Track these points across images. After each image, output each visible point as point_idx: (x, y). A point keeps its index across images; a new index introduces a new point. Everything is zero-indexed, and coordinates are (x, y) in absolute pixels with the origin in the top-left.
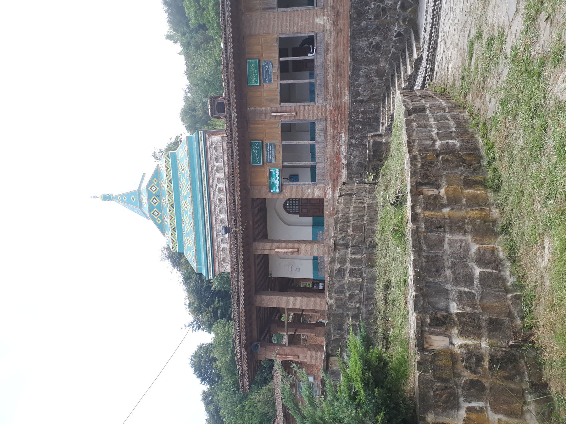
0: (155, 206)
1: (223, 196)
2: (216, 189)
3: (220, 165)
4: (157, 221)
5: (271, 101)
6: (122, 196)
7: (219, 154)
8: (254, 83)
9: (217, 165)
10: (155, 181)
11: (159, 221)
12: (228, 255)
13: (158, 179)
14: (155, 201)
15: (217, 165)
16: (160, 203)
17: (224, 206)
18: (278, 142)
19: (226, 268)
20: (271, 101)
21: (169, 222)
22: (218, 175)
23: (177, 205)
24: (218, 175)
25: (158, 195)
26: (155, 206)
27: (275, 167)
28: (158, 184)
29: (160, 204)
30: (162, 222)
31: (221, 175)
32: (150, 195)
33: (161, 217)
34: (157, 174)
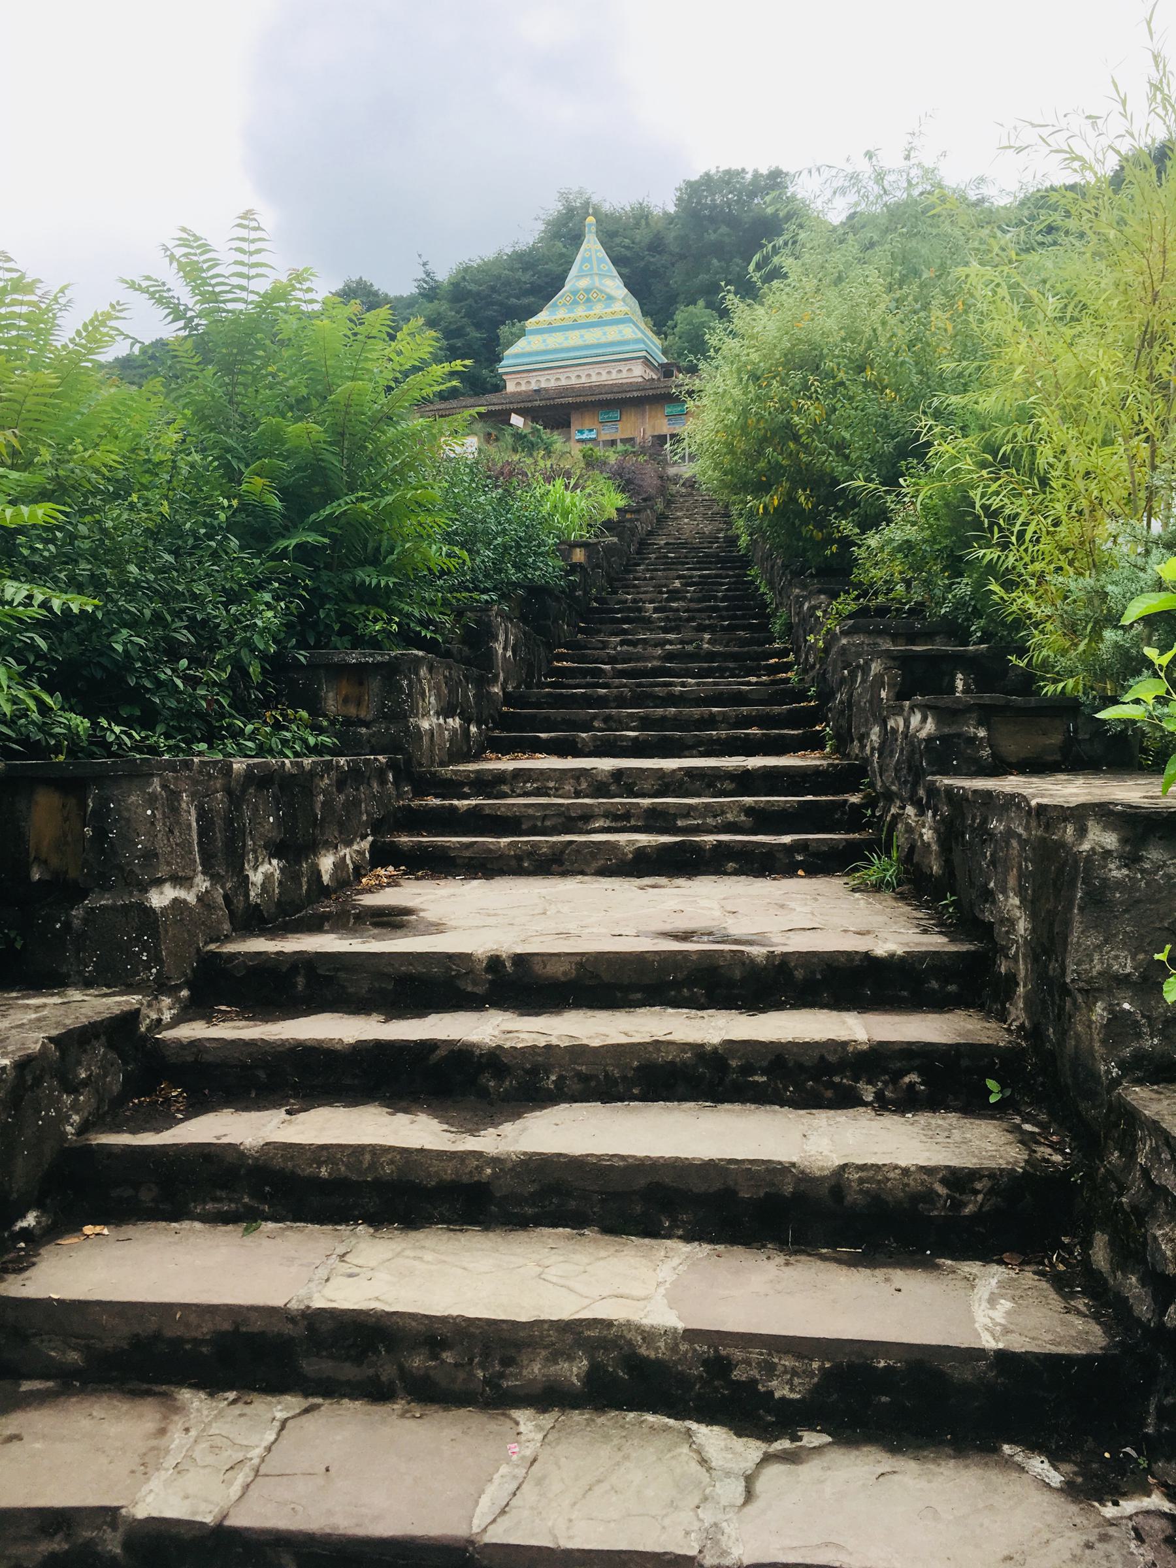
1: (583, 380)
2: (591, 372)
3: (614, 375)
5: (654, 427)
7: (625, 374)
8: (668, 410)
9: (614, 372)
12: (523, 388)
15: (614, 372)
17: (574, 381)
18: (618, 436)
19: (511, 387)
20: (654, 427)
22: (604, 373)
24: (604, 373)
27: (597, 433)
29: (578, 303)
31: (604, 377)
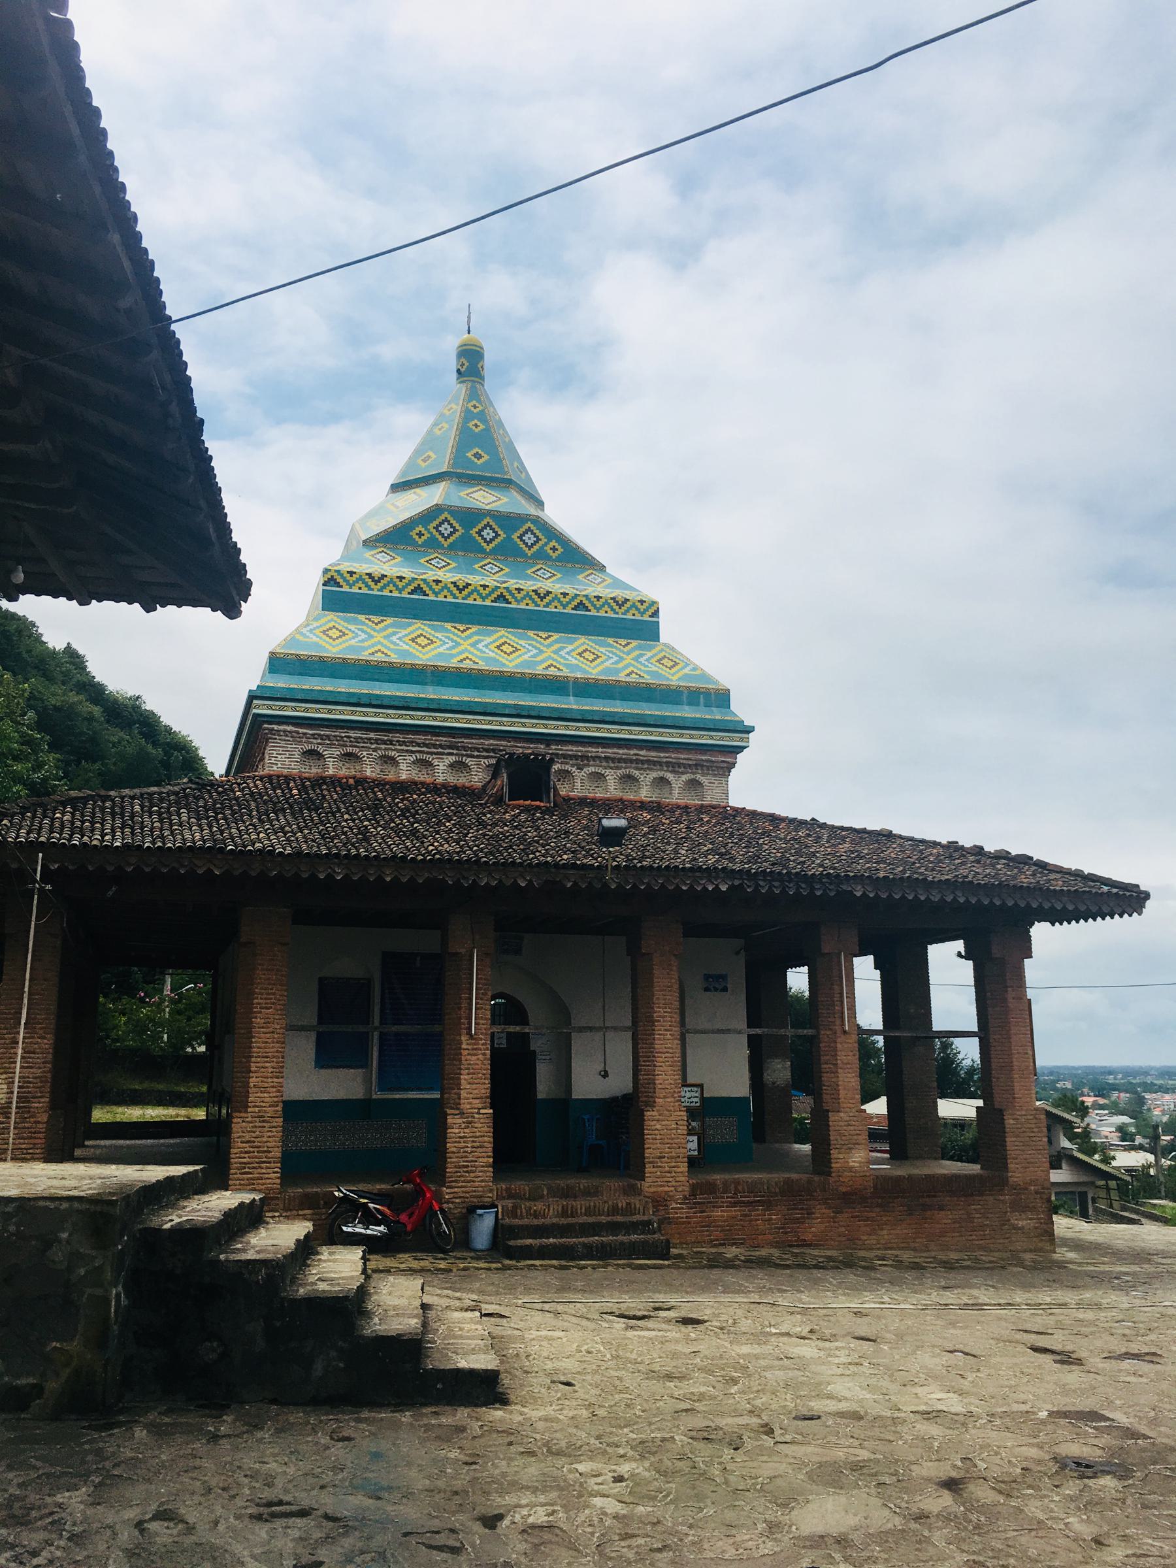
0: (515, 537)
4: (420, 528)
6: (483, 417)
10: (554, 549)
11: (420, 534)
13: (558, 559)
14: (488, 534)
16: (483, 551)
21: (529, 585)
23: (496, 613)
25: (508, 552)
26: (515, 537)
28: (541, 556)
30: (414, 543)
32: (509, 521)
33: (432, 544)
34: (575, 558)
